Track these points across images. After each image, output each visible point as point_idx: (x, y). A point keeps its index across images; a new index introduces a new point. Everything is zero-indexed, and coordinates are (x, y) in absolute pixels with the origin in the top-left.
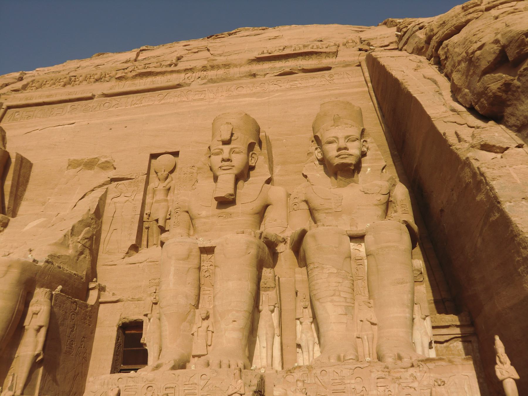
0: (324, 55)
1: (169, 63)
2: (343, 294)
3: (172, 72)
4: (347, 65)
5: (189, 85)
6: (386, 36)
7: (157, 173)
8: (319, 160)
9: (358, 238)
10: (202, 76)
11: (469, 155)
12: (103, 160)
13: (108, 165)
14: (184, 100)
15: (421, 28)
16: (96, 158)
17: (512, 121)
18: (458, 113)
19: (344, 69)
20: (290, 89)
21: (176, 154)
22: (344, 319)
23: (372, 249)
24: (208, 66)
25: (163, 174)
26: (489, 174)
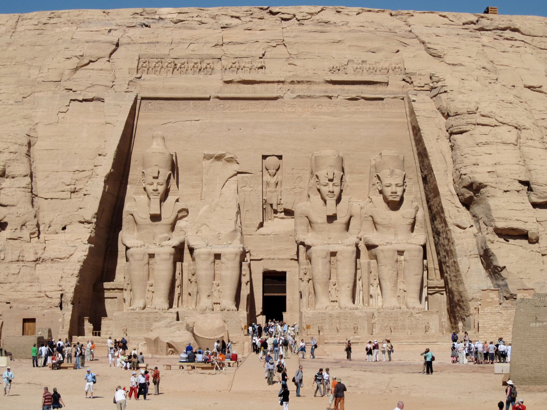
0: (379, 85)
1: (260, 65)
2: (394, 278)
4: (395, 98)
5: (282, 97)
6: (423, 72)
7: (267, 170)
9: (401, 253)
10: (291, 89)
13: (232, 160)
15: (445, 92)
17: (471, 210)
21: (280, 157)
22: (393, 288)
23: (407, 258)
24: (295, 79)
25: (273, 171)
26: (456, 242)
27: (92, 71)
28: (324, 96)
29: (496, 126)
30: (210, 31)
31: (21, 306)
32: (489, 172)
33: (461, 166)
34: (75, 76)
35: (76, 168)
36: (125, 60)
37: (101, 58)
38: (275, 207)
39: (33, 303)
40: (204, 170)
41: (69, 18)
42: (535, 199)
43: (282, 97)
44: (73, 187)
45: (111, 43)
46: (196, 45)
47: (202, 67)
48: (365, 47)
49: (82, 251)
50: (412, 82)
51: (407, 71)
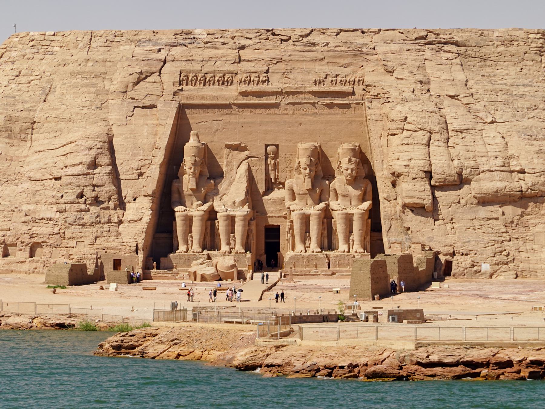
15: (389, 102)
20: (330, 114)
21: (277, 146)
27: (148, 84)
29: (415, 131)
30: (230, 51)
31: (112, 251)
32: (405, 166)
34: (136, 87)
35: (141, 157)
36: (170, 74)
37: (155, 73)
38: (273, 181)
39: (120, 249)
40: (225, 156)
41: (128, 37)
42: (433, 182)
44: (139, 171)
45: (160, 60)
46: (220, 62)
47: (225, 80)
48: (338, 63)
49: (147, 216)
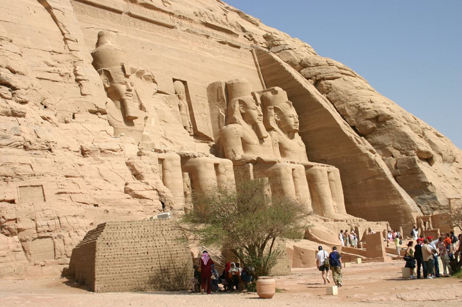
0: (234, 35)
3: (163, 11)
4: (246, 49)
8: (276, 120)
11: (368, 152)
12: (147, 73)
13: (150, 78)
14: (178, 40)
15: (289, 49)
16: (143, 71)
17: (370, 140)
18: (348, 127)
19: (245, 50)
20: (224, 54)
21: (185, 83)
23: (334, 178)
28: (204, 35)
29: (355, 77)
32: (387, 108)
33: (357, 102)
43: (176, 28)
50: (253, 39)
51: (247, 29)
